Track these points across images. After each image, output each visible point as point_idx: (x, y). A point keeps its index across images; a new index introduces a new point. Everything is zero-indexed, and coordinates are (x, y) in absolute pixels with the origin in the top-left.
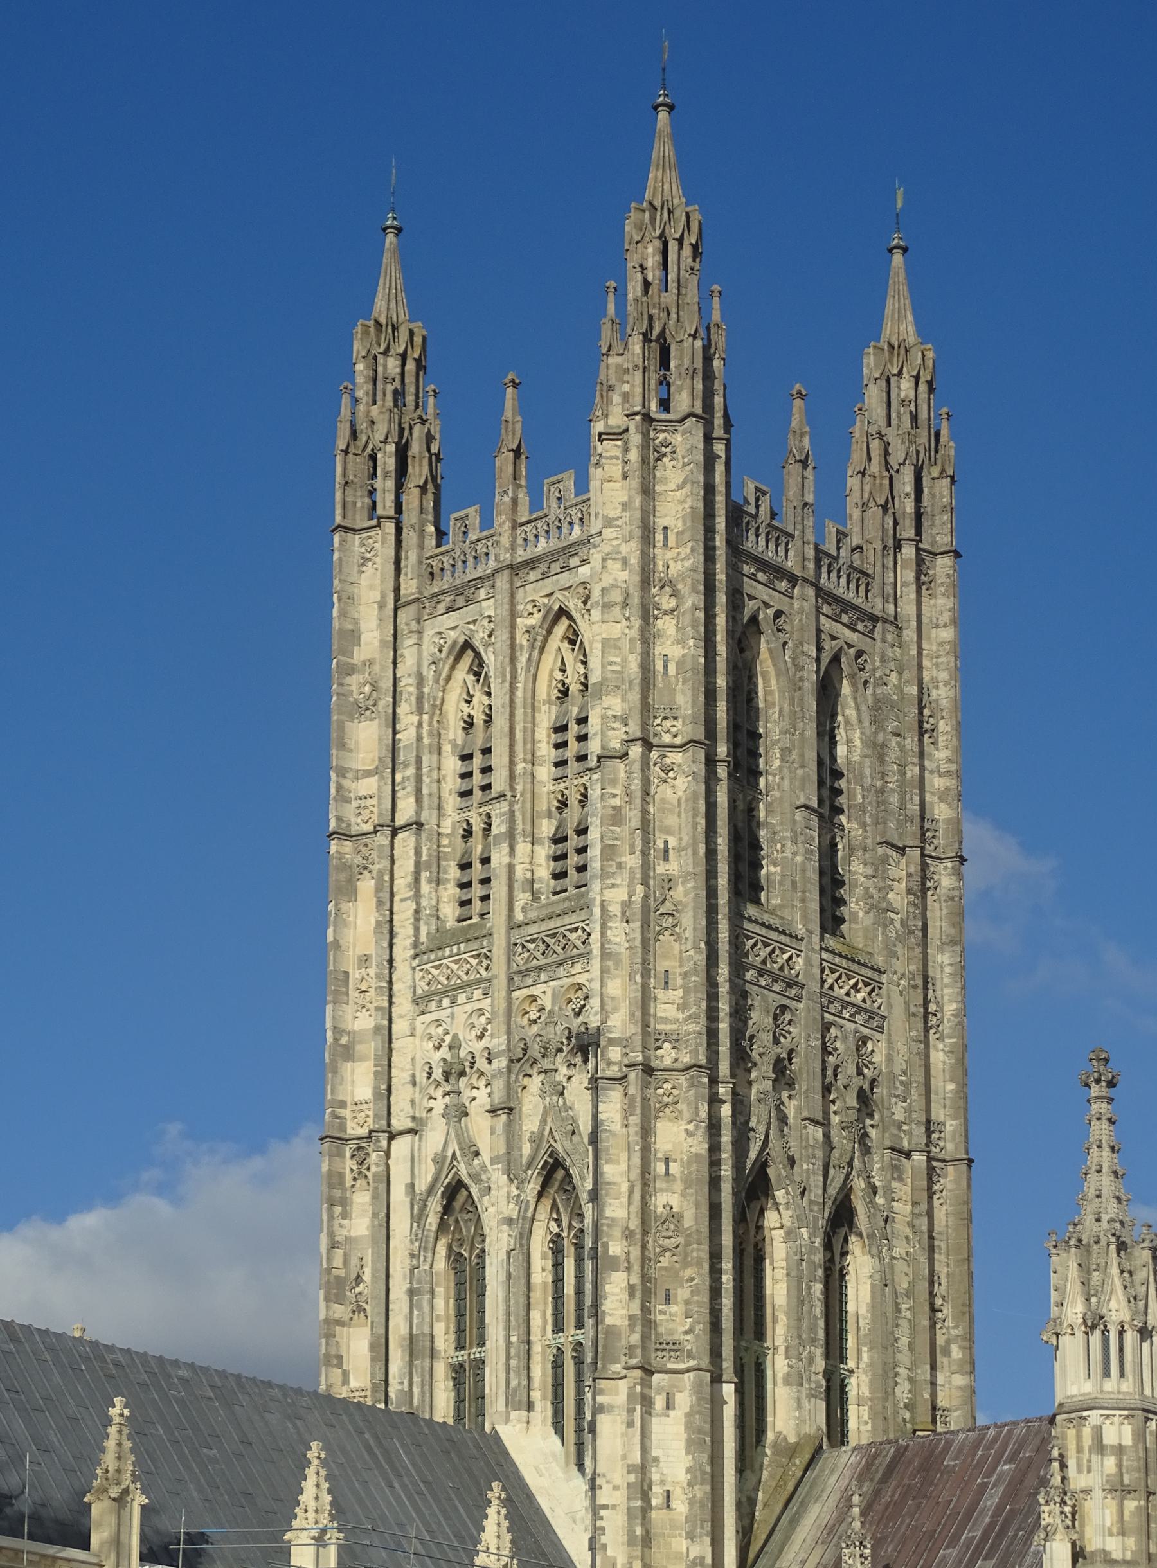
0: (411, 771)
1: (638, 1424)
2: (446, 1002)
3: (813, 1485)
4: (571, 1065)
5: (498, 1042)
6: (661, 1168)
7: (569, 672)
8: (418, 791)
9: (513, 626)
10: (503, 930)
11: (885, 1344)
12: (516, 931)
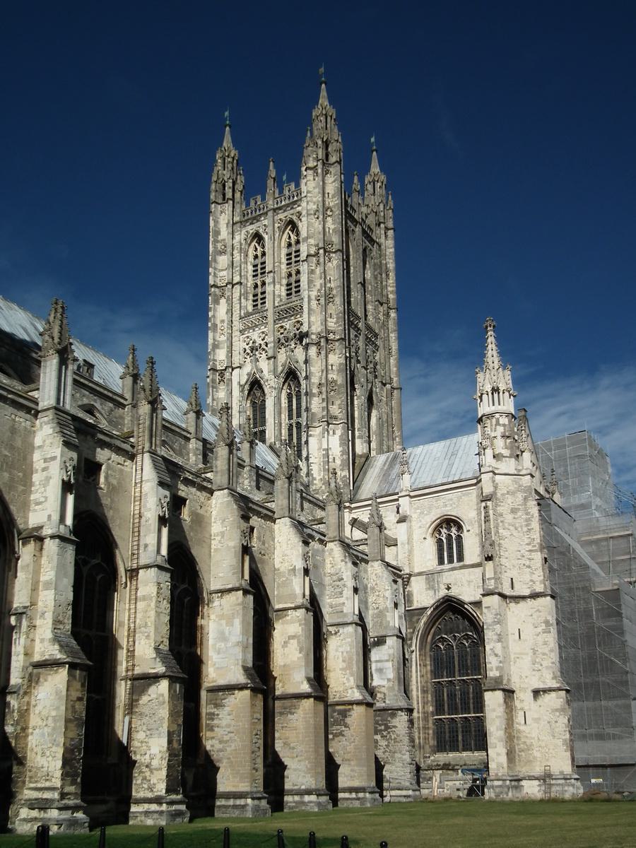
0: (238, 268)
1: (326, 437)
2: (251, 331)
3: (369, 464)
4: (296, 344)
5: (269, 339)
8: (241, 274)
10: (272, 308)
11: (380, 435)
12: (277, 309)
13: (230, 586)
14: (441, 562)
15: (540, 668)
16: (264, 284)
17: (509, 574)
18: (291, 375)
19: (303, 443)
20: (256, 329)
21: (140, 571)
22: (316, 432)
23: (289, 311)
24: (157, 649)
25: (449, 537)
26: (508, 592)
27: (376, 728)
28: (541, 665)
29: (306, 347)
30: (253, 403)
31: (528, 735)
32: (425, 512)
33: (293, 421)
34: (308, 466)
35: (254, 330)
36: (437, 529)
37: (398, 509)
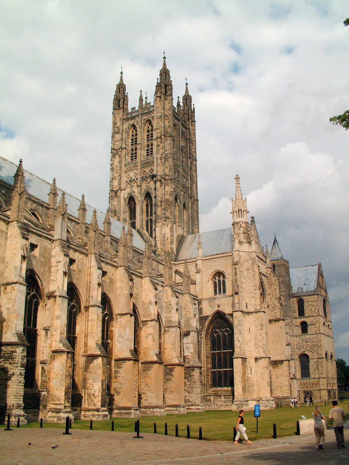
0: (125, 141)
2: (130, 172)
3: (184, 240)
4: (150, 180)
5: (139, 177)
6: (166, 193)
7: (149, 128)
9: (141, 122)
10: (140, 162)
13: (124, 312)
14: (216, 293)
15: (258, 347)
16: (136, 149)
17: (245, 301)
18: (148, 196)
19: (153, 230)
20: (133, 171)
21: (90, 308)
22: (159, 225)
23: (147, 164)
24: (97, 344)
25: (219, 281)
27: (185, 376)
28: (259, 345)
29: (155, 182)
30: (130, 208)
31: (252, 379)
32: (209, 268)
33: (149, 218)
34: (155, 242)
35: (131, 172)
36: (214, 277)
37: (196, 266)
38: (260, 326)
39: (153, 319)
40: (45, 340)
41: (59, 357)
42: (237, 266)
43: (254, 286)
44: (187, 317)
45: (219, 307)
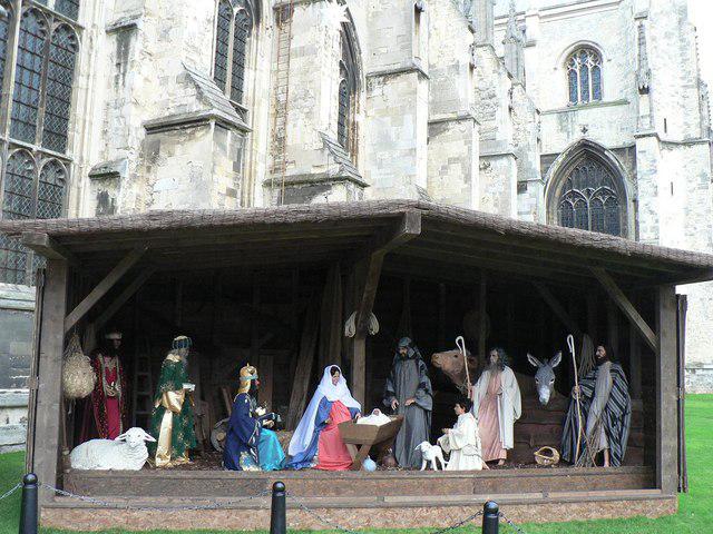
13: (398, 67)
14: (573, 98)
15: (693, 231)
26: (663, 137)
36: (570, 59)
38: (699, 179)
39: (463, 114)
40: (117, 77)
41: (178, 149)
42: (644, 22)
43: (683, 78)
44: (517, 145)
45: (585, 130)
